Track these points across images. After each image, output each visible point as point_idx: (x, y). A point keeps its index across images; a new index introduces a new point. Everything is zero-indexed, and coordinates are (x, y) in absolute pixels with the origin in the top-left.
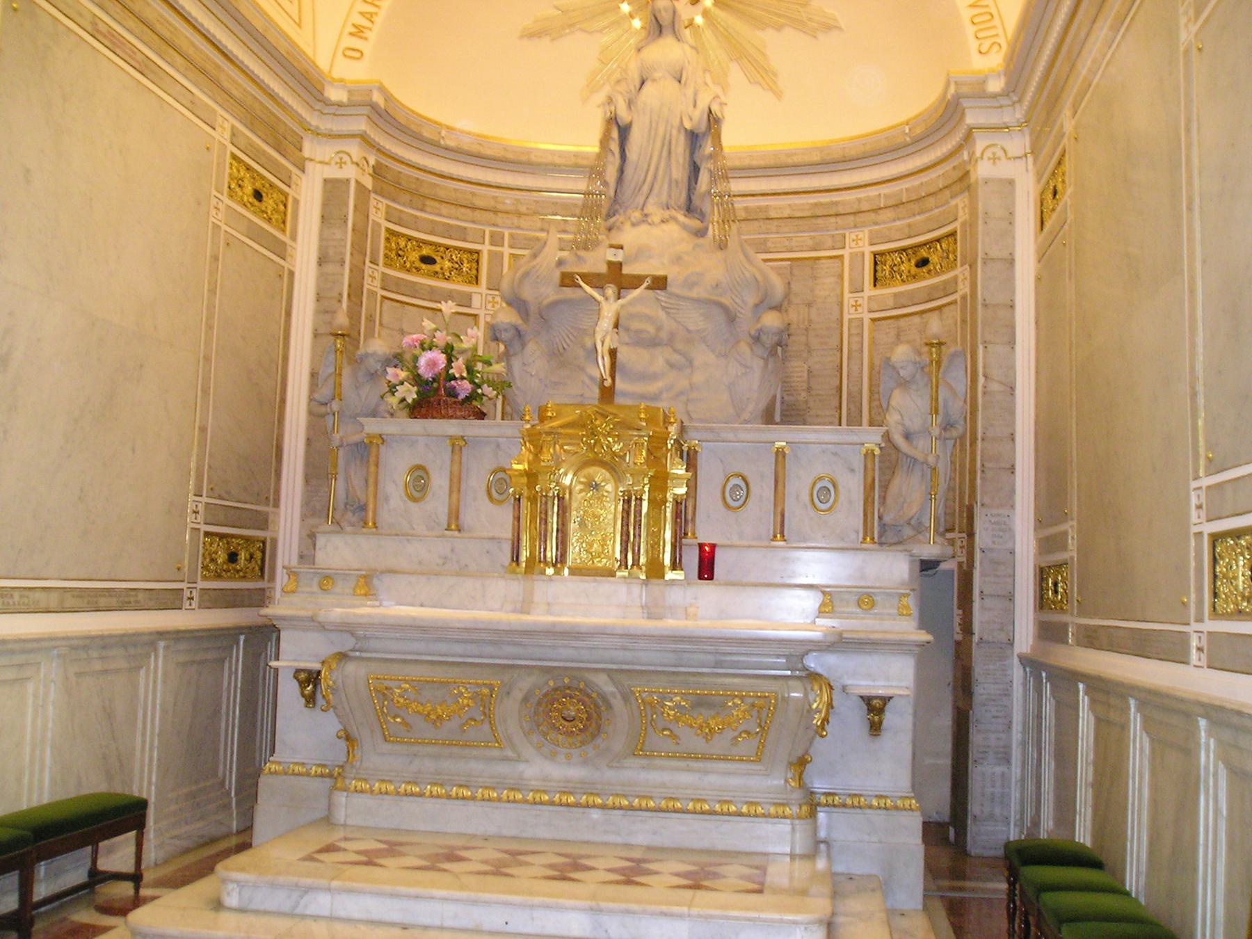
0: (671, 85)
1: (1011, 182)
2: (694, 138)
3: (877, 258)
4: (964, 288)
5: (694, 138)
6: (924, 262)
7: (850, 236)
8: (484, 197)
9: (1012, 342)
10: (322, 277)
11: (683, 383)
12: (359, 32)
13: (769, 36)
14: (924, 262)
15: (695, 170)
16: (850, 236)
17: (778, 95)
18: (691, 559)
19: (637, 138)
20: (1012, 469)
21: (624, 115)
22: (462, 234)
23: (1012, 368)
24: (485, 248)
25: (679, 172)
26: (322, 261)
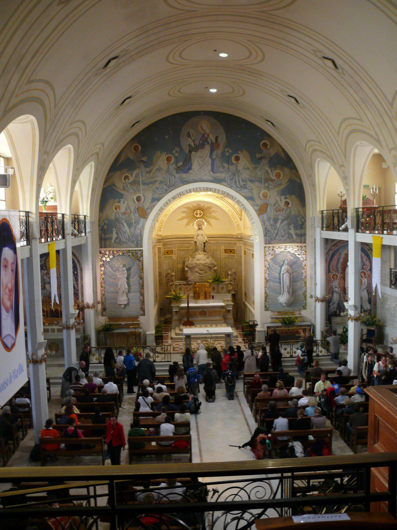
0: (201, 236)
1: (241, 247)
2: (204, 243)
3: (225, 249)
4: (236, 257)
5: (204, 243)
6: (231, 251)
7: (222, 246)
8: (173, 242)
9: (241, 265)
10: (159, 260)
11: (206, 275)
12: (160, 228)
13: (210, 219)
14: (231, 251)
15: (204, 246)
16: (222, 246)
17: (211, 226)
18: (211, 297)
19: (197, 243)
20: (242, 280)
21: (196, 241)
22: (170, 248)
23: (241, 268)
24: (174, 249)
25: (203, 247)
26: (159, 258)
